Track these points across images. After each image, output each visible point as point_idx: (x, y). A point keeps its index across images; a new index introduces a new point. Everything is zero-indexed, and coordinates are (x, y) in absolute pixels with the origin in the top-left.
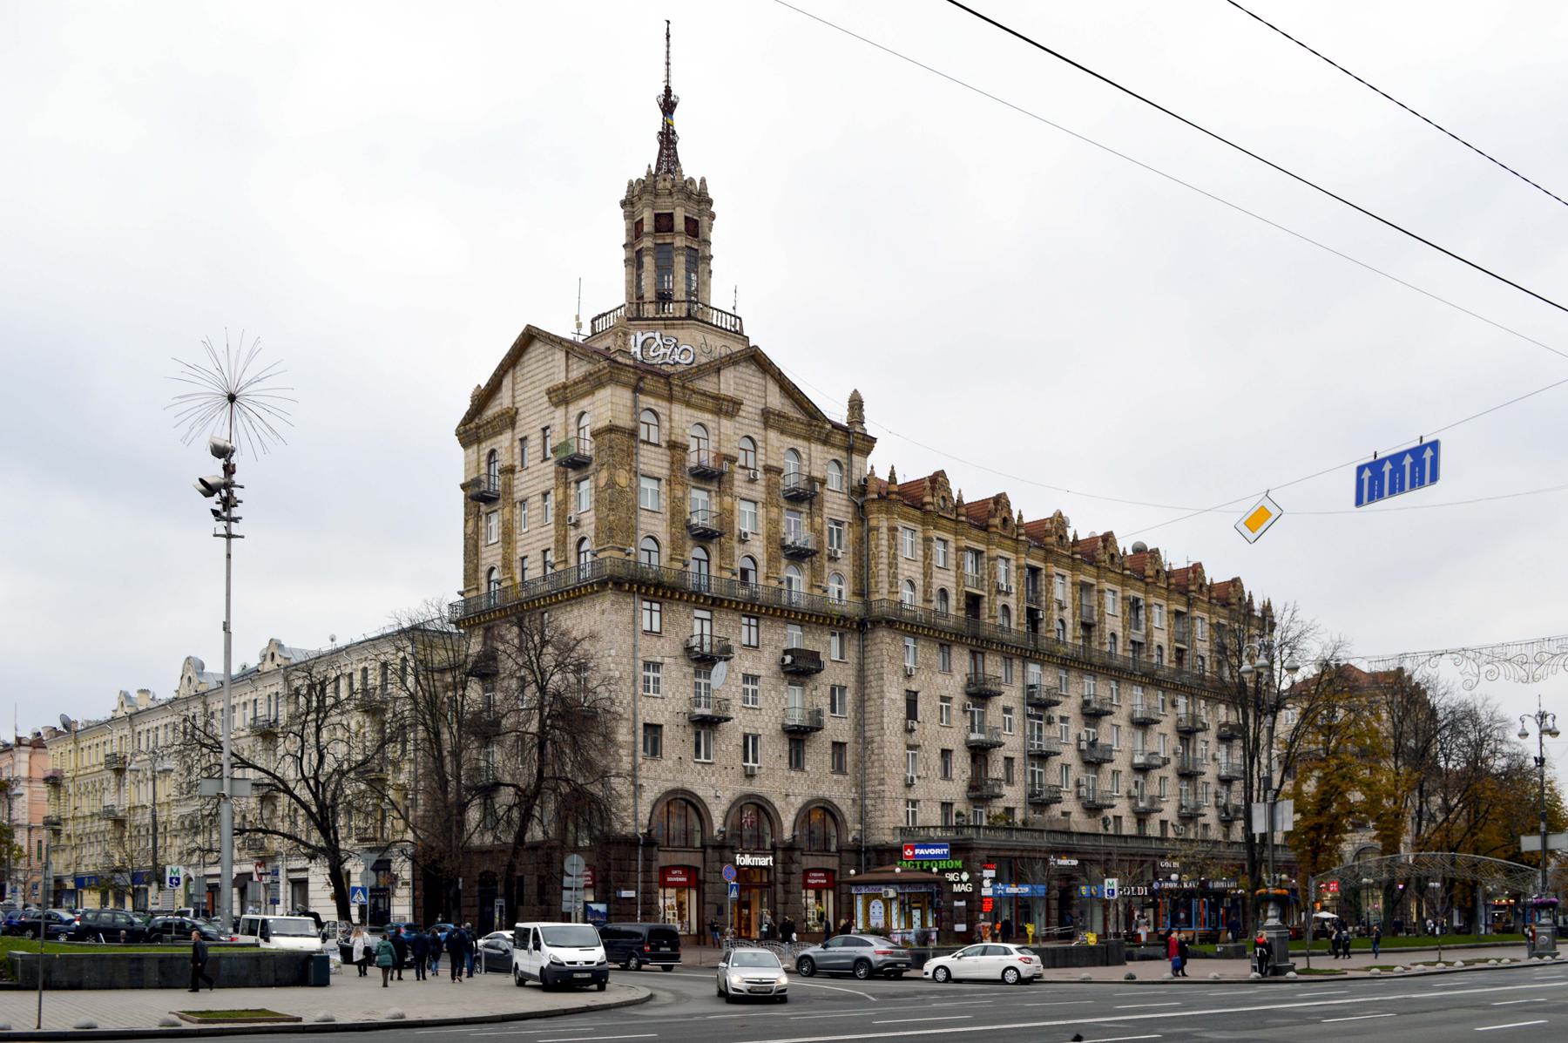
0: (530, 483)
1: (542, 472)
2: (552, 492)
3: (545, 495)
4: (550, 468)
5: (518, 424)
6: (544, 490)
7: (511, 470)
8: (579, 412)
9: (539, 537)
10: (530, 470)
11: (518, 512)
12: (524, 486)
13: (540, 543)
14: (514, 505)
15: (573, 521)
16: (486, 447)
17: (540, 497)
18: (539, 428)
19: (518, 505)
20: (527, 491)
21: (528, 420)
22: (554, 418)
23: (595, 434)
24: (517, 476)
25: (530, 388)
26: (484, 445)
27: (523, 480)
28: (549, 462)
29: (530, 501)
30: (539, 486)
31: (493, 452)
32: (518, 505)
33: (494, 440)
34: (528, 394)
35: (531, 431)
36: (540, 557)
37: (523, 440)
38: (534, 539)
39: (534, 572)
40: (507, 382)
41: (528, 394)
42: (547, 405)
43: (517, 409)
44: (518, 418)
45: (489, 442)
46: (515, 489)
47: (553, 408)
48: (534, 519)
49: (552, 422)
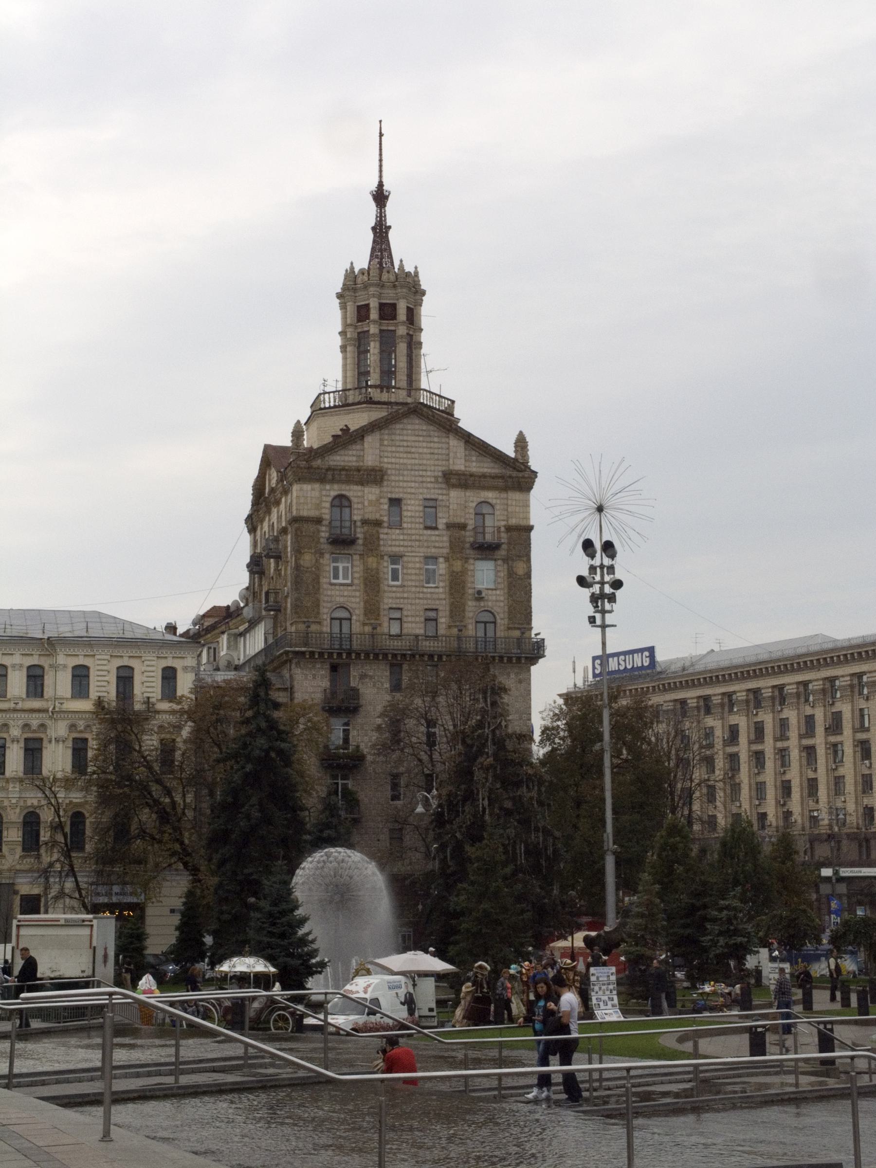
0: (406, 543)
1: (425, 538)
2: (441, 560)
3: (431, 559)
4: (440, 541)
5: (385, 483)
6: (429, 555)
7: (378, 523)
8: (479, 500)
9: (421, 595)
10: (405, 532)
11: (385, 564)
12: (397, 543)
13: (421, 601)
14: (382, 557)
15: (483, 595)
16: (334, 490)
17: (422, 559)
18: (421, 497)
19: (386, 558)
20: (402, 549)
21: (401, 484)
22: (443, 495)
23: (509, 529)
24: (382, 531)
25: (405, 456)
26: (328, 487)
27: (394, 537)
28: (437, 532)
29: (405, 559)
30: (422, 550)
31: (341, 497)
32: (386, 558)
33: (344, 487)
34: (401, 461)
35: (409, 496)
36: (422, 613)
37: (395, 502)
38: (413, 596)
39: (415, 626)
40: (371, 441)
41: (401, 461)
42: (433, 480)
43: (387, 469)
44: (386, 477)
45: (336, 486)
46: (382, 543)
47: (443, 486)
48: (413, 577)
49: (440, 497)
